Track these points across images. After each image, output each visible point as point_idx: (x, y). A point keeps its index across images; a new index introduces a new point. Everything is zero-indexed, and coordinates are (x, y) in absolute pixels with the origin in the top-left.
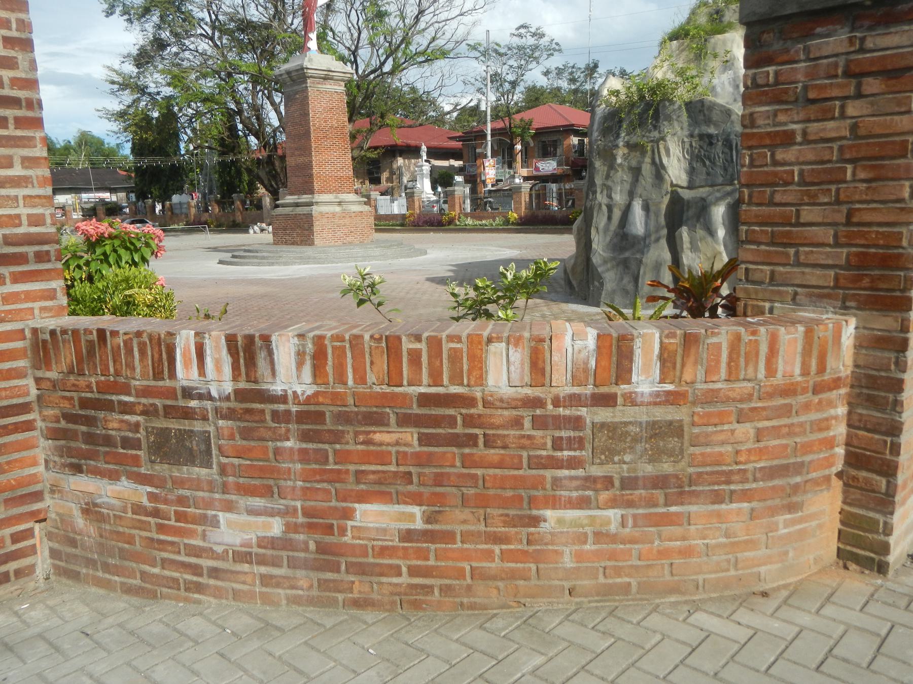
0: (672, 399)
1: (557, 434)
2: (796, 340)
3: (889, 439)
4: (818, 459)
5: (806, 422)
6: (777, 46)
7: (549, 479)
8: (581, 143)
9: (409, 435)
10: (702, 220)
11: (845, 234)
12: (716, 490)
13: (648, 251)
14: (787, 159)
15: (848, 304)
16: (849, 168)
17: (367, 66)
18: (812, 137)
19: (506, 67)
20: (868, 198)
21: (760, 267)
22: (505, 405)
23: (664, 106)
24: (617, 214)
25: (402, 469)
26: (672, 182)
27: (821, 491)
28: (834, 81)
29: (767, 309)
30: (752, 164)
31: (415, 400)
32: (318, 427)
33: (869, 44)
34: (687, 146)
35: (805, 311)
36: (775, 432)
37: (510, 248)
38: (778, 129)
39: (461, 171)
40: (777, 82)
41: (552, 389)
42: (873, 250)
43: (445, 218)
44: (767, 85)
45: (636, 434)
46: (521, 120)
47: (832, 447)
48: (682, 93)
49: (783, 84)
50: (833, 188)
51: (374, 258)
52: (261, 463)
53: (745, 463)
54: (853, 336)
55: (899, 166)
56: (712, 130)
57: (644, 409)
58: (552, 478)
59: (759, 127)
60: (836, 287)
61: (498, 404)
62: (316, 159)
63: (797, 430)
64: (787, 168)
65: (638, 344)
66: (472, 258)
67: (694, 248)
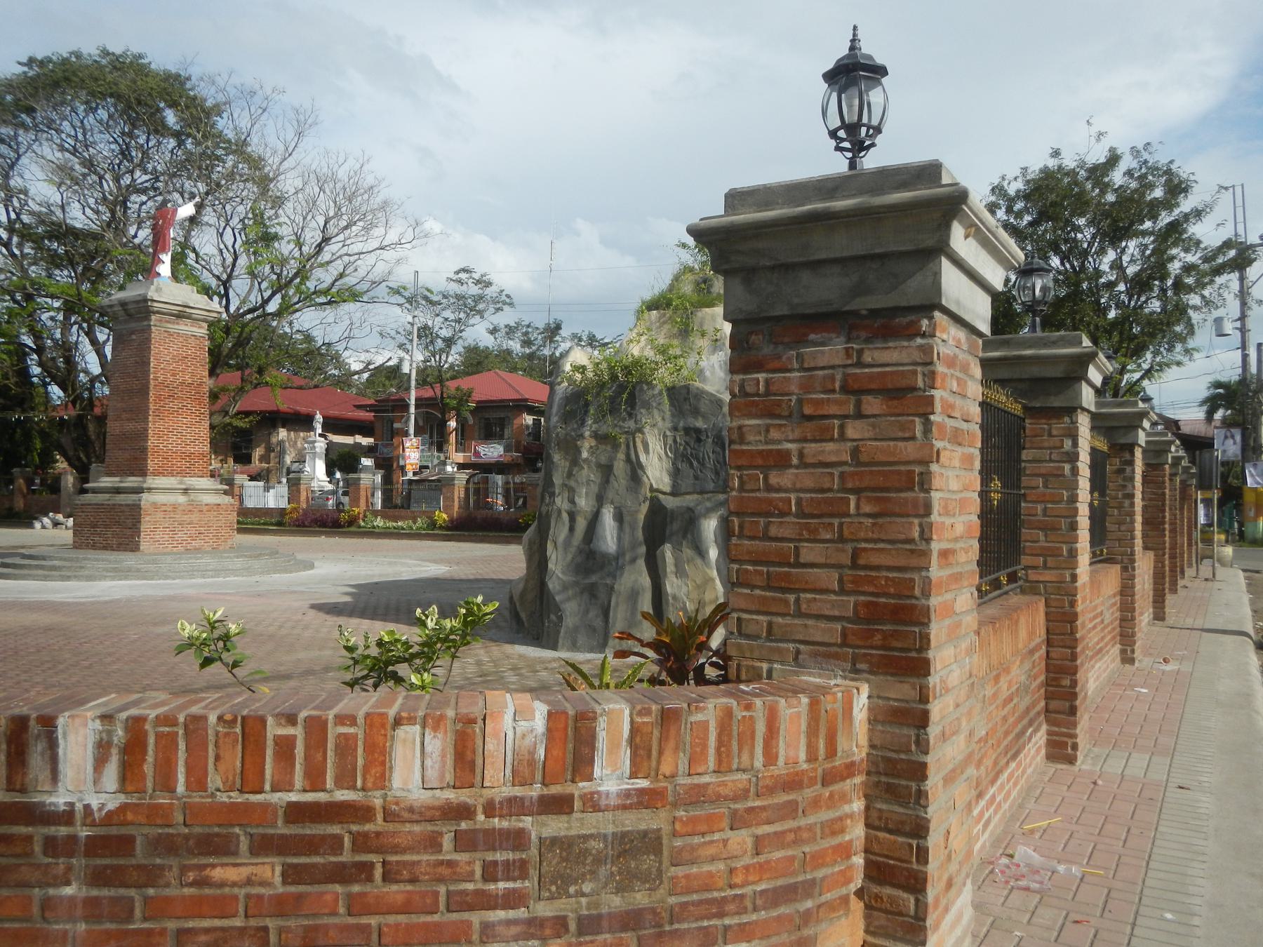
0: (646, 800)
1: (490, 857)
2: (799, 714)
3: (914, 843)
4: (833, 874)
5: (816, 824)
6: (767, 350)
7: (476, 926)
8: (537, 423)
9: (268, 869)
10: (689, 536)
11: (851, 578)
12: (706, 928)
13: (622, 575)
14: (782, 484)
15: (859, 666)
16: (853, 499)
17: (243, 302)
18: (809, 460)
19: (439, 319)
20: (875, 536)
21: (755, 617)
22: (415, 817)
23: (642, 390)
24: (581, 524)
25: (253, 922)
26: (651, 485)
27: (839, 918)
28: (831, 396)
29: (765, 671)
30: (742, 488)
31: (280, 813)
32: (122, 862)
33: (867, 358)
34: (670, 441)
35: (810, 674)
36: (778, 839)
37: (435, 561)
38: (770, 447)
39: (369, 451)
40: (768, 393)
41: (485, 791)
42: (883, 600)
43: (344, 517)
44: (758, 395)
45: (599, 852)
46: (457, 389)
47: (849, 857)
48: (664, 376)
49: (775, 395)
50: (836, 522)
51: (234, 572)
52: (17, 925)
53: (742, 886)
54: (866, 706)
55: (906, 499)
56: (700, 424)
57: (609, 815)
58: (481, 923)
59: (749, 443)
60: (844, 644)
61: (406, 815)
62: (154, 426)
63: (805, 835)
64: (784, 495)
65: (602, 723)
66: (380, 575)
67: (680, 572)
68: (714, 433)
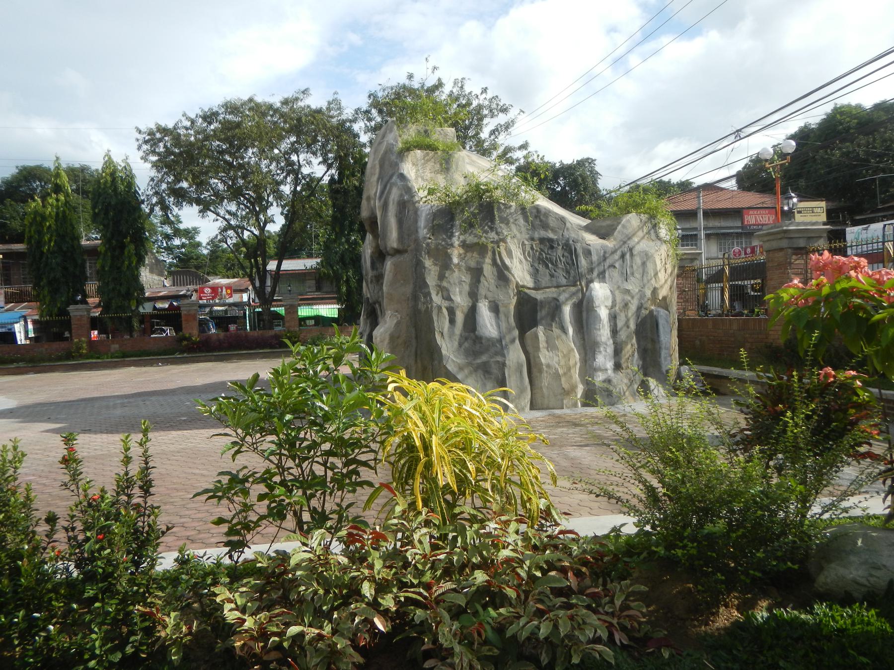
13: (508, 353)
24: (460, 317)
34: (528, 248)
56: (551, 235)
67: (551, 346)
68: (563, 242)
